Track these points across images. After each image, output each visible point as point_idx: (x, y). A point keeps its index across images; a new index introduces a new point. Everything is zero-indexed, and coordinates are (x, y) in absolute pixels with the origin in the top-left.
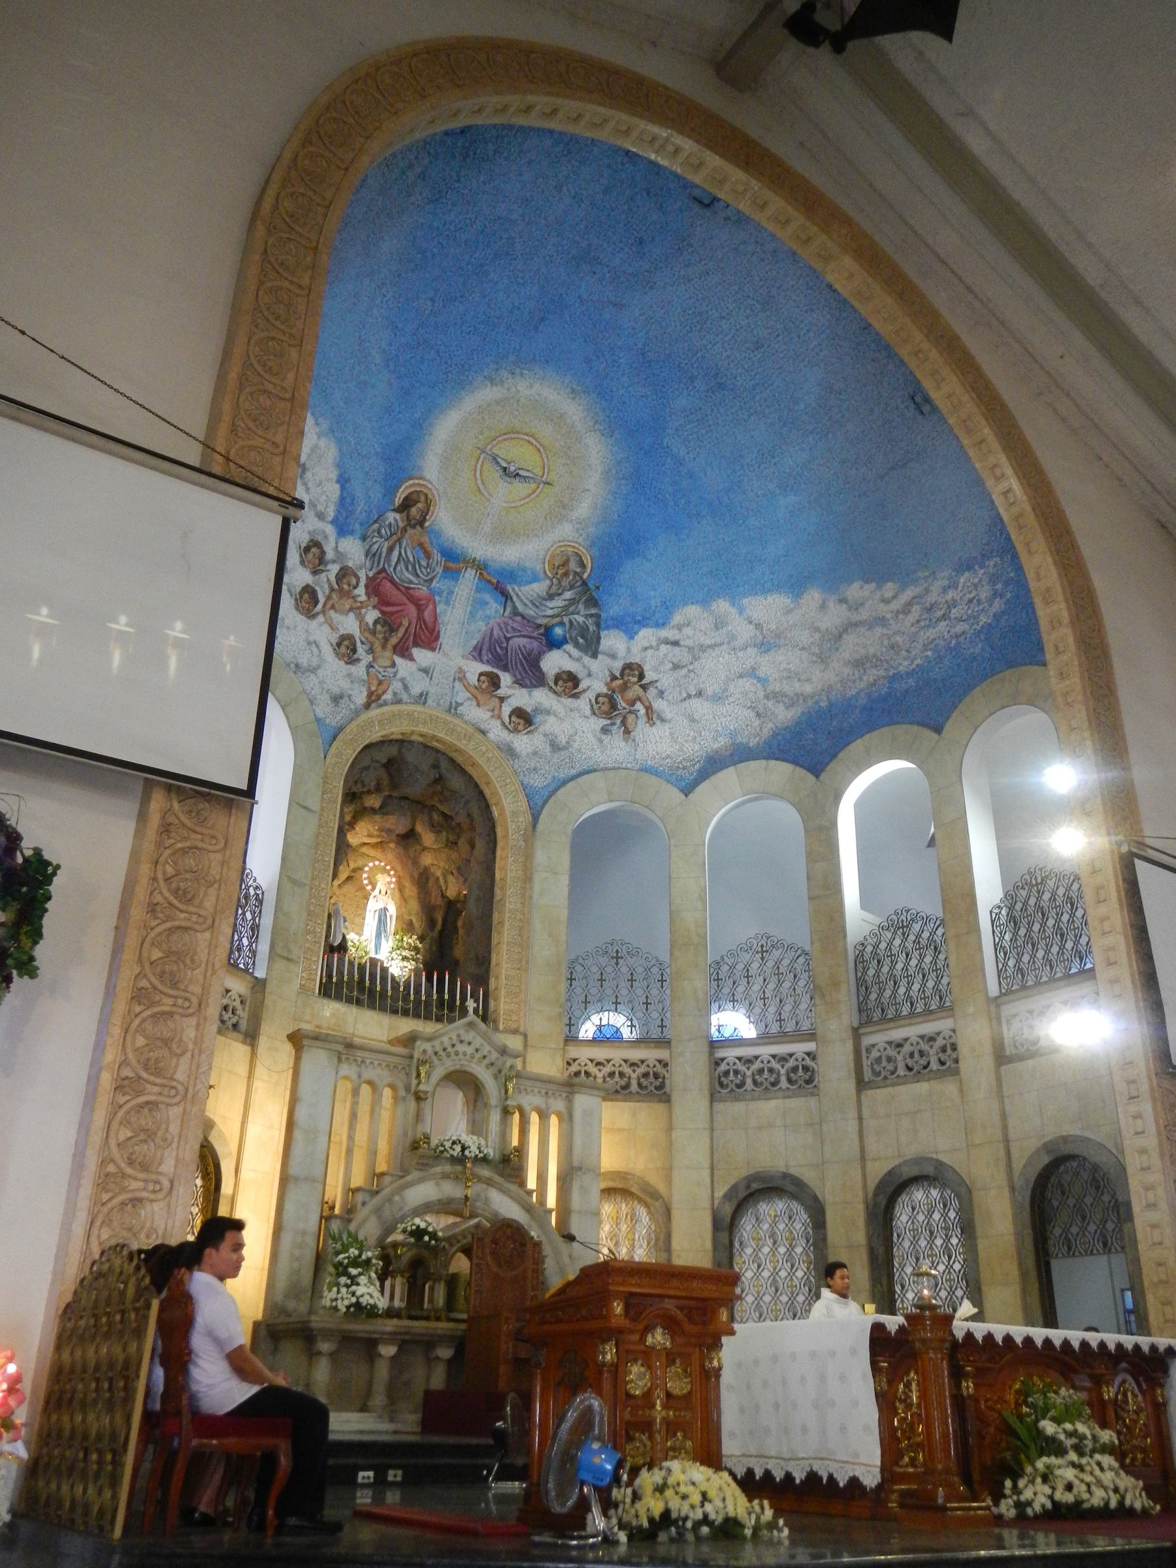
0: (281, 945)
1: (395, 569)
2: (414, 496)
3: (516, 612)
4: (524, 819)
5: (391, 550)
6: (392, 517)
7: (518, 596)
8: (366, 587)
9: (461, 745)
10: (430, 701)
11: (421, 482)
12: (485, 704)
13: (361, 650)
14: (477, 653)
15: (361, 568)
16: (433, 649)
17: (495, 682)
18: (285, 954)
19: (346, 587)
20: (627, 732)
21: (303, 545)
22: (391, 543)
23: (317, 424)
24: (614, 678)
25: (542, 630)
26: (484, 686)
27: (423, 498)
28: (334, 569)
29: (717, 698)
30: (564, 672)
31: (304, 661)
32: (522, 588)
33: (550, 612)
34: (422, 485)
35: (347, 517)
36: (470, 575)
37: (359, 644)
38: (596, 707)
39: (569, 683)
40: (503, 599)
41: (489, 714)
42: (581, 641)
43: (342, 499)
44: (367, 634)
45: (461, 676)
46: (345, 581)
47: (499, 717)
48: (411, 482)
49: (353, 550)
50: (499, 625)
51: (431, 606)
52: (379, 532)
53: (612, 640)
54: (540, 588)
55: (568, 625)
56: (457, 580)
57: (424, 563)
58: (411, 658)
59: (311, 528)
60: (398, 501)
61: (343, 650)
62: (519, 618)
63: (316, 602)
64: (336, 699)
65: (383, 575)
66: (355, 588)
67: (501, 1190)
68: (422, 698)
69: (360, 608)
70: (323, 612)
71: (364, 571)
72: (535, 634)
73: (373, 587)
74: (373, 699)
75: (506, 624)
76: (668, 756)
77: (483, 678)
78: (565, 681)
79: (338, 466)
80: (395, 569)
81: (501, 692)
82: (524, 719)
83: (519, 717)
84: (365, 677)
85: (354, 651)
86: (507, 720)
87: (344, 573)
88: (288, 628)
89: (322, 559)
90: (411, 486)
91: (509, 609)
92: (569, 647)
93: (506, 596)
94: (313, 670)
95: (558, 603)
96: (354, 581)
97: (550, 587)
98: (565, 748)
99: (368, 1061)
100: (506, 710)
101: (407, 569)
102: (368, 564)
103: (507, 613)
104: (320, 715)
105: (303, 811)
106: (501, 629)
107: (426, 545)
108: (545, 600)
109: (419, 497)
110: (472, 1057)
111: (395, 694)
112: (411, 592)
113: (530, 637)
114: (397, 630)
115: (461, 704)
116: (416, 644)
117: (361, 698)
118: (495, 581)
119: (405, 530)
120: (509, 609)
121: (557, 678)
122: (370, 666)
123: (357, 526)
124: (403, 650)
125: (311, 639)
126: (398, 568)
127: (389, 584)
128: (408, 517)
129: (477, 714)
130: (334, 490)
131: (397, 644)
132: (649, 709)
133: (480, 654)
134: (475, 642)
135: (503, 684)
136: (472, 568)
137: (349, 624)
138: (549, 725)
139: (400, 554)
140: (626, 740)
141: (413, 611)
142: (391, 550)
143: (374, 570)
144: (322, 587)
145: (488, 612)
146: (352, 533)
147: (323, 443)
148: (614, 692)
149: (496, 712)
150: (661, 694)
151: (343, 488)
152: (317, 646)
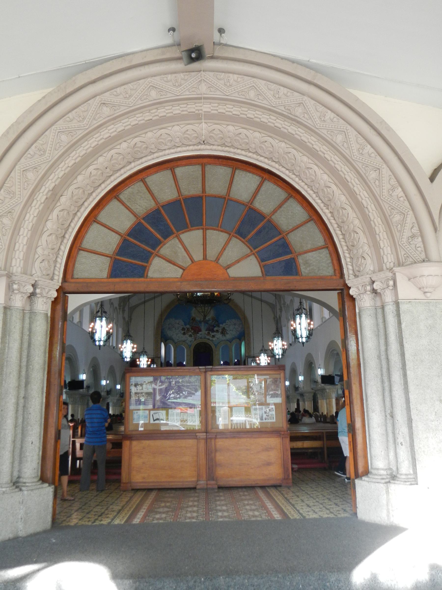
14: (206, 330)
17: (209, 333)
29: (232, 331)
39: (217, 331)
45: (205, 333)
49: (188, 326)
53: (221, 325)
64: (191, 342)
68: (201, 338)
73: (192, 329)
74: (195, 339)
82: (213, 336)
95: (213, 323)
117: (194, 340)
129: (208, 337)
137: (190, 333)
138: (216, 336)
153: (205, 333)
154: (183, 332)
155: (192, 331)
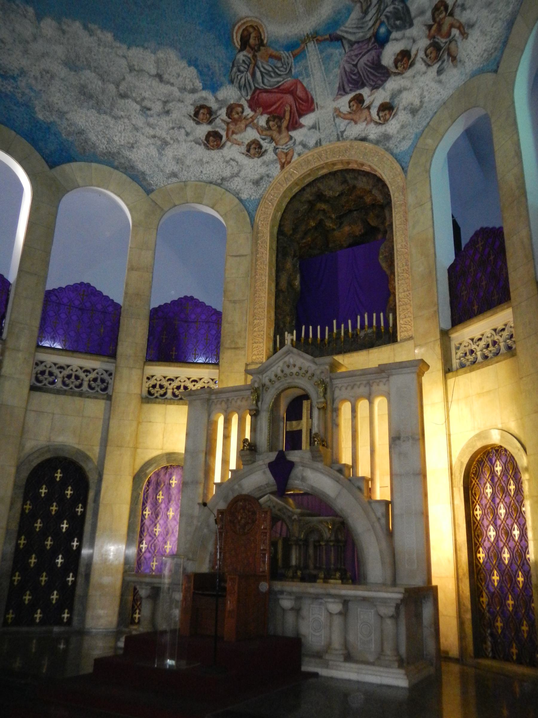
0: (229, 341)
1: (263, 83)
2: (246, 33)
3: (352, 44)
4: (400, 180)
5: (253, 75)
6: (241, 57)
7: (347, 32)
8: (250, 106)
9: (346, 158)
10: (324, 143)
11: (242, 22)
12: (360, 118)
13: (264, 144)
14: (342, 91)
15: (240, 99)
16: (313, 110)
17: (359, 99)
18: (233, 346)
19: (236, 116)
20: (454, 59)
21: (192, 113)
22: (251, 70)
23: (146, 48)
24: (430, 27)
25: (373, 40)
26: (354, 108)
27: (251, 30)
28: (223, 112)
30: (398, 55)
31: (227, 173)
32: (347, 25)
33: (371, 23)
34: (244, 23)
35: (212, 79)
36: (312, 48)
37: (262, 142)
38: (428, 60)
40: (340, 43)
41: (365, 123)
42: (398, 22)
43: (201, 73)
44: (264, 133)
45: (338, 113)
46: (234, 113)
47: (372, 120)
48: (236, 27)
50: (347, 61)
51: (299, 86)
52: (239, 71)
54: (356, 14)
55: (385, 20)
56: (305, 57)
57: (279, 65)
58: (301, 126)
59: (191, 102)
60: (237, 44)
61: (252, 151)
62: (356, 46)
63: (221, 137)
64: (257, 183)
65: (258, 92)
66: (242, 112)
67: (313, 469)
68: (319, 143)
69: (252, 121)
70: (228, 139)
71: (243, 99)
72: (370, 47)
73: (254, 104)
75: (349, 57)
76: (485, 50)
77: (351, 104)
78: (401, 60)
79: (182, 58)
80: (263, 83)
81: (366, 103)
83: (383, 110)
84: (276, 157)
85: (260, 147)
86: (377, 118)
87: (230, 110)
88: (208, 163)
89: (210, 112)
90: (239, 28)
91: (346, 46)
92: (395, 35)
93: (339, 39)
94: (237, 175)
95: (373, 11)
96: (240, 109)
97: (362, 7)
98: (421, 106)
99: (230, 399)
100: (374, 112)
101: (271, 77)
102: (244, 93)
103: (347, 50)
104: (244, 196)
105: (238, 258)
106: (349, 63)
107: (274, 54)
108: (364, 17)
109: (248, 31)
110: (298, 374)
111: (299, 155)
112: (281, 88)
113: (368, 51)
114: (284, 117)
115: (345, 130)
116: (301, 115)
117: (275, 170)
118: (327, 36)
119: (255, 56)
120: (346, 46)
121: (396, 62)
122: (275, 149)
123: (223, 79)
124: (294, 125)
125: (228, 159)
126: (266, 81)
127: (264, 95)
128: (250, 47)
130: (192, 71)
131: (288, 125)
132: (461, 27)
133: (344, 90)
134: (337, 85)
135: (365, 97)
136: (310, 41)
137: (251, 134)
139: (261, 72)
140: (455, 66)
141: (289, 98)
142: (253, 75)
143: (250, 94)
144: (220, 127)
145: (336, 59)
146: (221, 85)
147: (161, 55)
148: (434, 37)
149: (368, 119)
150: (463, 7)
151: (196, 66)
152: (233, 160)
153: (338, 113)
154: (203, 130)
155: (262, 121)
